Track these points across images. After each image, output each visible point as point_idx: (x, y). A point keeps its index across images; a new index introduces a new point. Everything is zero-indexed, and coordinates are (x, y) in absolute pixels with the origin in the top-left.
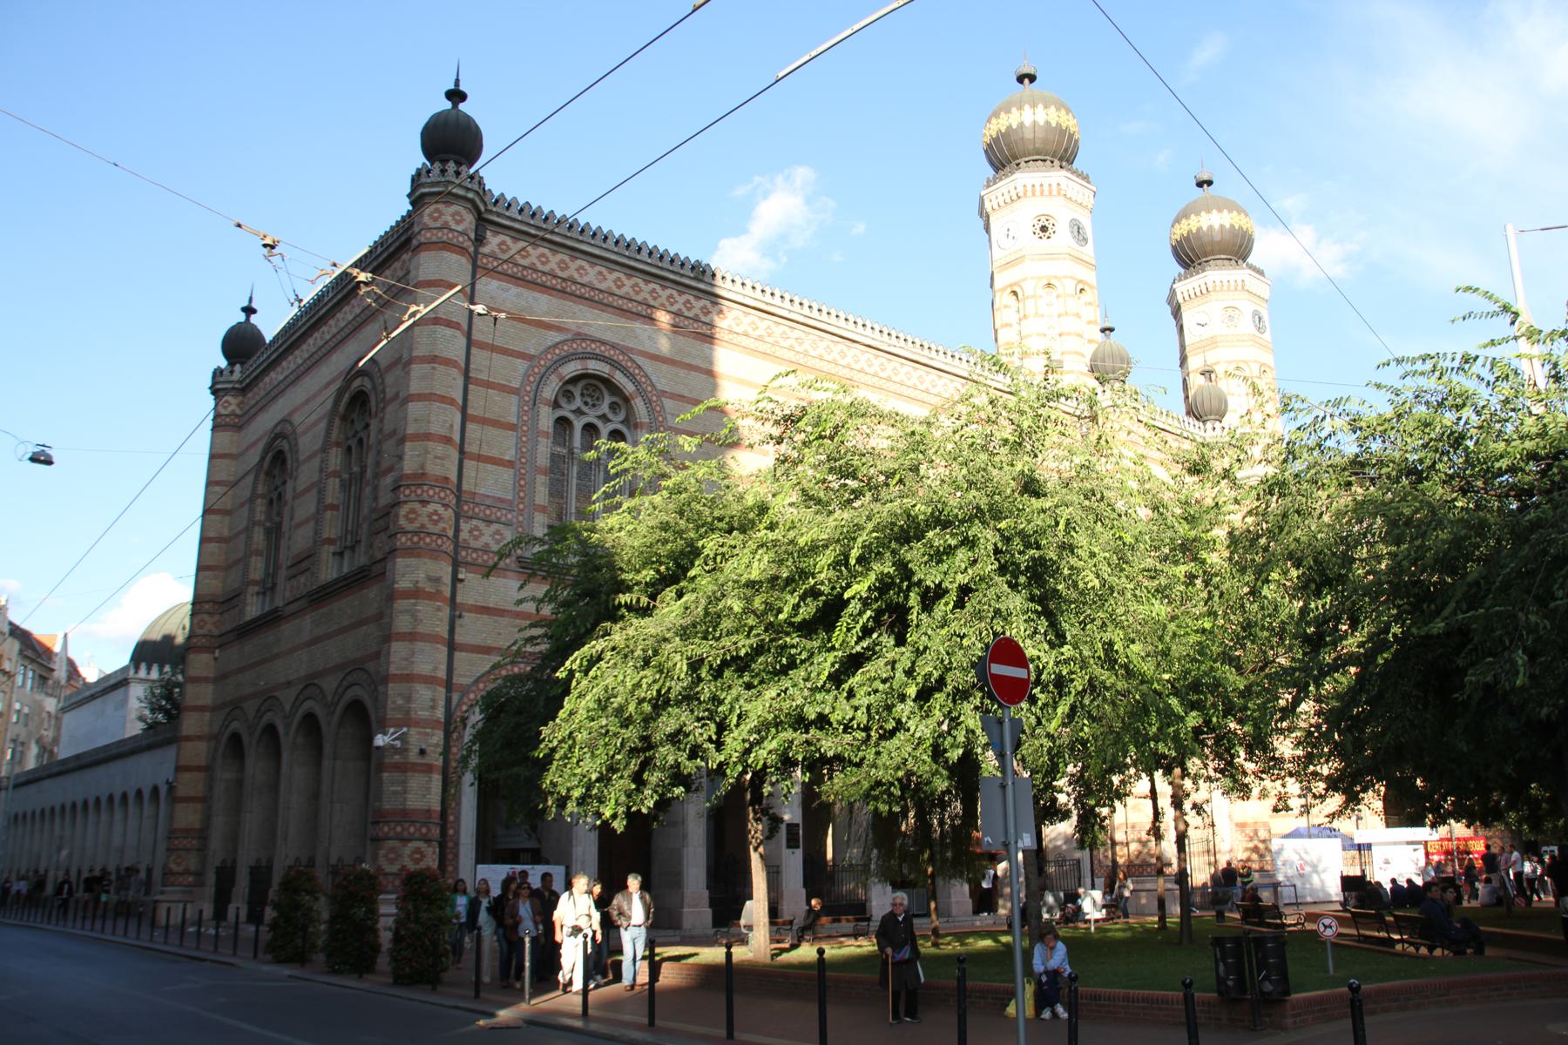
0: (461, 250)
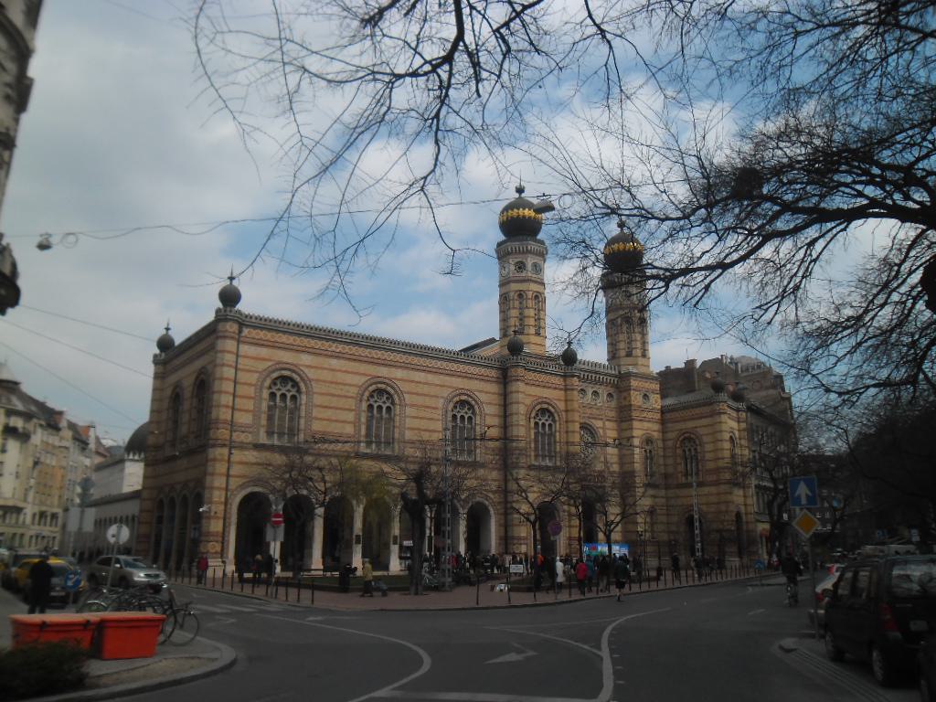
0: (232, 338)
